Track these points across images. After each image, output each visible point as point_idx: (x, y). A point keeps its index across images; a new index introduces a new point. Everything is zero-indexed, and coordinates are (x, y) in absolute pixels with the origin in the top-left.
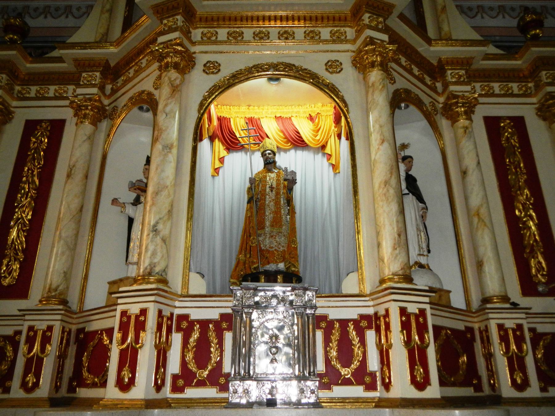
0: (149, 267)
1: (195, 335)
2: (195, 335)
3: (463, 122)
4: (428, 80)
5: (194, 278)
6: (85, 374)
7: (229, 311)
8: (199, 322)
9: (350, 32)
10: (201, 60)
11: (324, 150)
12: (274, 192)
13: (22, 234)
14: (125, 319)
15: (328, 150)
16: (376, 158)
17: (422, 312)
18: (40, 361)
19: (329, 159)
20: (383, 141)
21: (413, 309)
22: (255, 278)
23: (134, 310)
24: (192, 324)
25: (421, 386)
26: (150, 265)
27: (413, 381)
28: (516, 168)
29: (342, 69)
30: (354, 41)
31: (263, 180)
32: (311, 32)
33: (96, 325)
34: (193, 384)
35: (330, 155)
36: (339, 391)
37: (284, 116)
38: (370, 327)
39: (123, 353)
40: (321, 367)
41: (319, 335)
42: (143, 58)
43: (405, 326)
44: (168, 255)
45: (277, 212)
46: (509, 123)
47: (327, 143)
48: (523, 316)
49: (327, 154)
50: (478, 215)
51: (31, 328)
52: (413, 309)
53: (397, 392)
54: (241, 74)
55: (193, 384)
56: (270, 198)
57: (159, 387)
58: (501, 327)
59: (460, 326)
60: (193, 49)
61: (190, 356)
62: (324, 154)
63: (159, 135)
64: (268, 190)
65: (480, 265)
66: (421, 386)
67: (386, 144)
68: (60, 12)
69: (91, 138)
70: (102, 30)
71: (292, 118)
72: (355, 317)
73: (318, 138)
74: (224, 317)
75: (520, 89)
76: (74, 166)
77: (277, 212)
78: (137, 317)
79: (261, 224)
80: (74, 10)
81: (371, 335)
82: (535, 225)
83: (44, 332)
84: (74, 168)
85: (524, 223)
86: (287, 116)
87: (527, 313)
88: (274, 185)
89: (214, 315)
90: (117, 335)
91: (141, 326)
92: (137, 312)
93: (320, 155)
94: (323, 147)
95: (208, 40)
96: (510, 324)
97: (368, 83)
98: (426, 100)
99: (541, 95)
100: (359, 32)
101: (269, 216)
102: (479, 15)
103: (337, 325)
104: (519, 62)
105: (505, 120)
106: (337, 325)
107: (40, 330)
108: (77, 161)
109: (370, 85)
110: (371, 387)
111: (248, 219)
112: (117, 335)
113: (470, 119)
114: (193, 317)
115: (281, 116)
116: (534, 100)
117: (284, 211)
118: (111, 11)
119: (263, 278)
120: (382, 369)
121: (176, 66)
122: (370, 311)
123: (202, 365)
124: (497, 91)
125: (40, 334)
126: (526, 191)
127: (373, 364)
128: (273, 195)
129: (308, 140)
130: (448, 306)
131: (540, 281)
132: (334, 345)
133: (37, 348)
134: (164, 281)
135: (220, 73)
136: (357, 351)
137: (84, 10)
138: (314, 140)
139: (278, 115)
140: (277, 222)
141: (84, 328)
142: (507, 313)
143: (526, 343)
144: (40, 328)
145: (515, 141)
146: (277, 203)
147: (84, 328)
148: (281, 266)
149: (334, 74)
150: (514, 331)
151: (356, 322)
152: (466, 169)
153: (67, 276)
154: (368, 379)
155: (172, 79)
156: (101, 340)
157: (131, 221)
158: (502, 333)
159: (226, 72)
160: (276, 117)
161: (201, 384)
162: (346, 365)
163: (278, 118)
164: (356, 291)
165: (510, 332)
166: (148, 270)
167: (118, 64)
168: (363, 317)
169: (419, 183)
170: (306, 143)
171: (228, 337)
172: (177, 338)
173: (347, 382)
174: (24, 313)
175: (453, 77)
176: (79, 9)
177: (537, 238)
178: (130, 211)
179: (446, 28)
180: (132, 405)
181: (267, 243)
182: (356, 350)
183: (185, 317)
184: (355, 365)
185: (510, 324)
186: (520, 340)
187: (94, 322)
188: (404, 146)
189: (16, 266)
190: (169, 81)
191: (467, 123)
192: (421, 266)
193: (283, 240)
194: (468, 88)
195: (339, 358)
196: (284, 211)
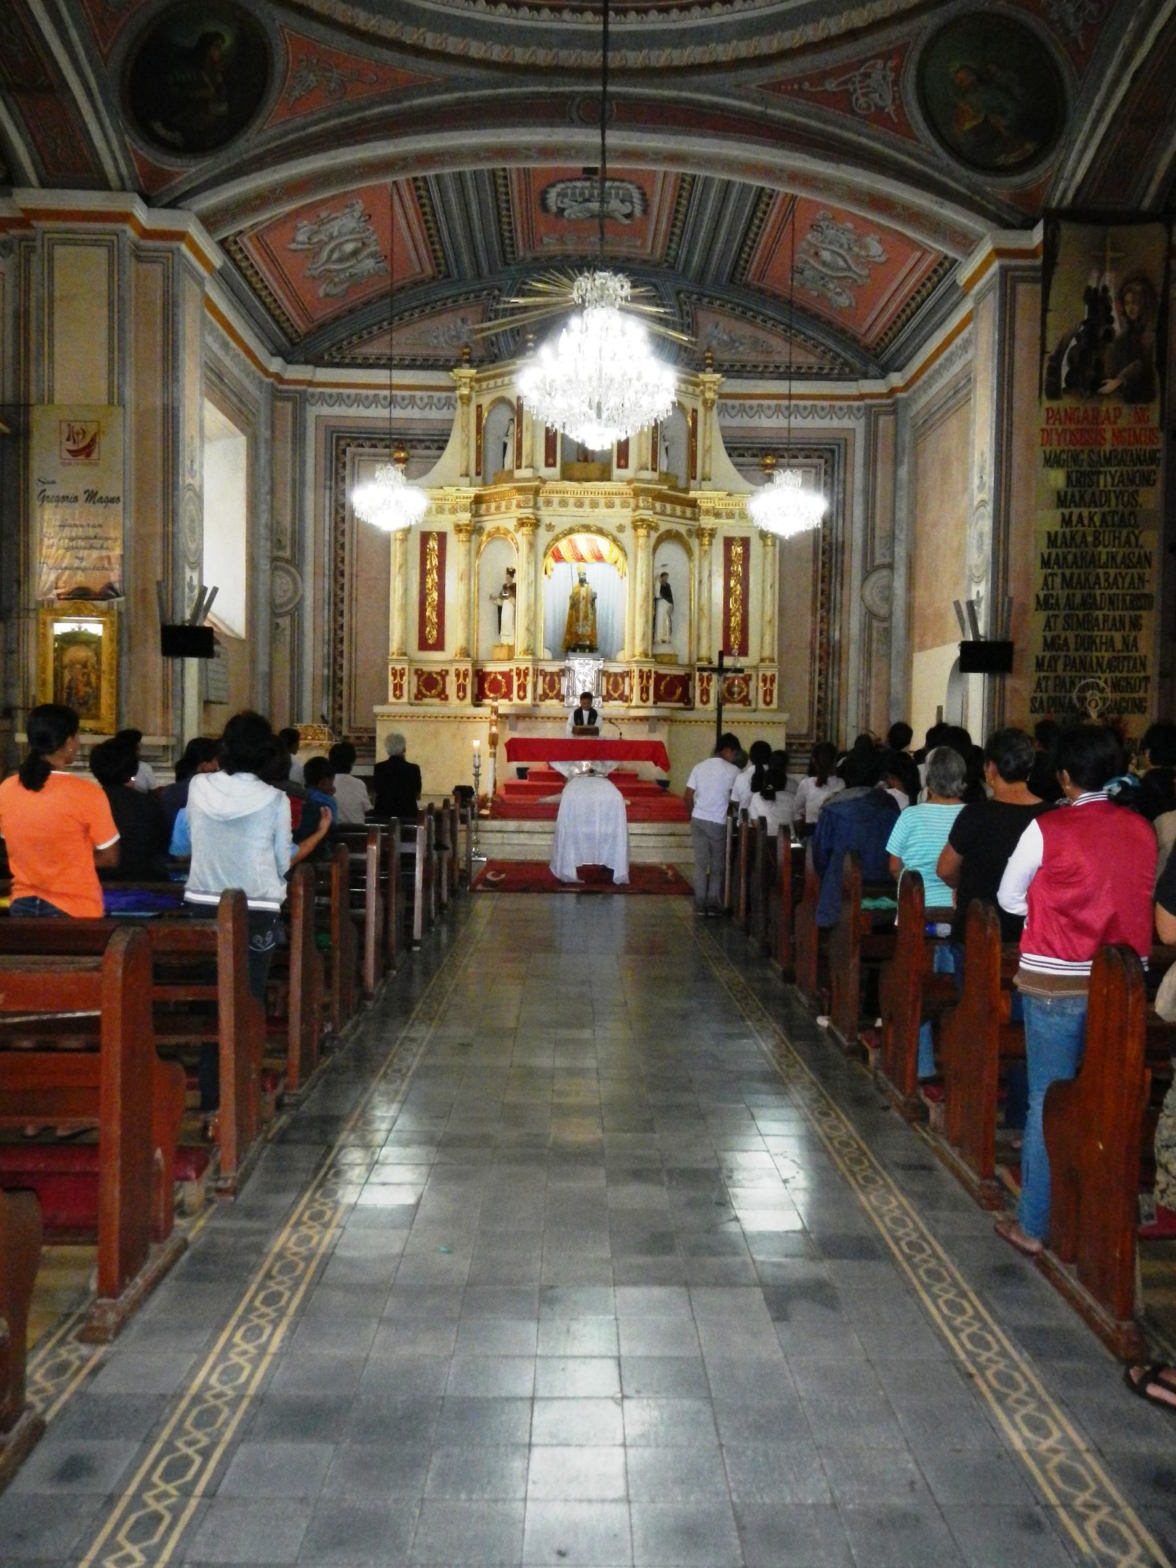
1: (548, 678)
3: (706, 548)
4: (688, 511)
5: (547, 651)
10: (546, 520)
13: (434, 614)
17: (650, 671)
21: (645, 669)
22: (574, 650)
23: (523, 667)
25: (644, 701)
27: (642, 698)
30: (634, 510)
31: (578, 593)
33: (490, 668)
36: (612, 703)
39: (519, 686)
40: (604, 693)
41: (605, 679)
43: (641, 677)
44: (535, 640)
45: (586, 612)
52: (645, 669)
53: (633, 704)
56: (582, 605)
57: (535, 699)
59: (682, 673)
60: (540, 513)
65: (699, 639)
66: (644, 701)
68: (407, 402)
69: (469, 551)
70: (464, 464)
77: (586, 612)
79: (577, 619)
80: (418, 402)
81: (627, 680)
90: (515, 678)
91: (526, 675)
95: (548, 503)
98: (683, 530)
100: (637, 507)
101: (582, 614)
102: (757, 417)
110: (626, 701)
111: (570, 616)
112: (515, 678)
113: (710, 544)
117: (590, 611)
118: (468, 445)
123: (552, 691)
127: (627, 692)
130: (676, 664)
134: (533, 654)
136: (621, 687)
137: (426, 400)
140: (586, 617)
146: (586, 606)
148: (588, 643)
153: (468, 640)
156: (495, 678)
157: (500, 609)
159: (557, 531)
162: (615, 691)
169: (673, 589)
172: (541, 679)
173: (615, 699)
174: (451, 662)
176: (421, 399)
178: (499, 602)
179: (707, 469)
180: (528, 708)
181: (580, 631)
183: (542, 670)
188: (664, 566)
189: (435, 632)
191: (706, 548)
192: (664, 642)
193: (589, 629)
196: (590, 611)
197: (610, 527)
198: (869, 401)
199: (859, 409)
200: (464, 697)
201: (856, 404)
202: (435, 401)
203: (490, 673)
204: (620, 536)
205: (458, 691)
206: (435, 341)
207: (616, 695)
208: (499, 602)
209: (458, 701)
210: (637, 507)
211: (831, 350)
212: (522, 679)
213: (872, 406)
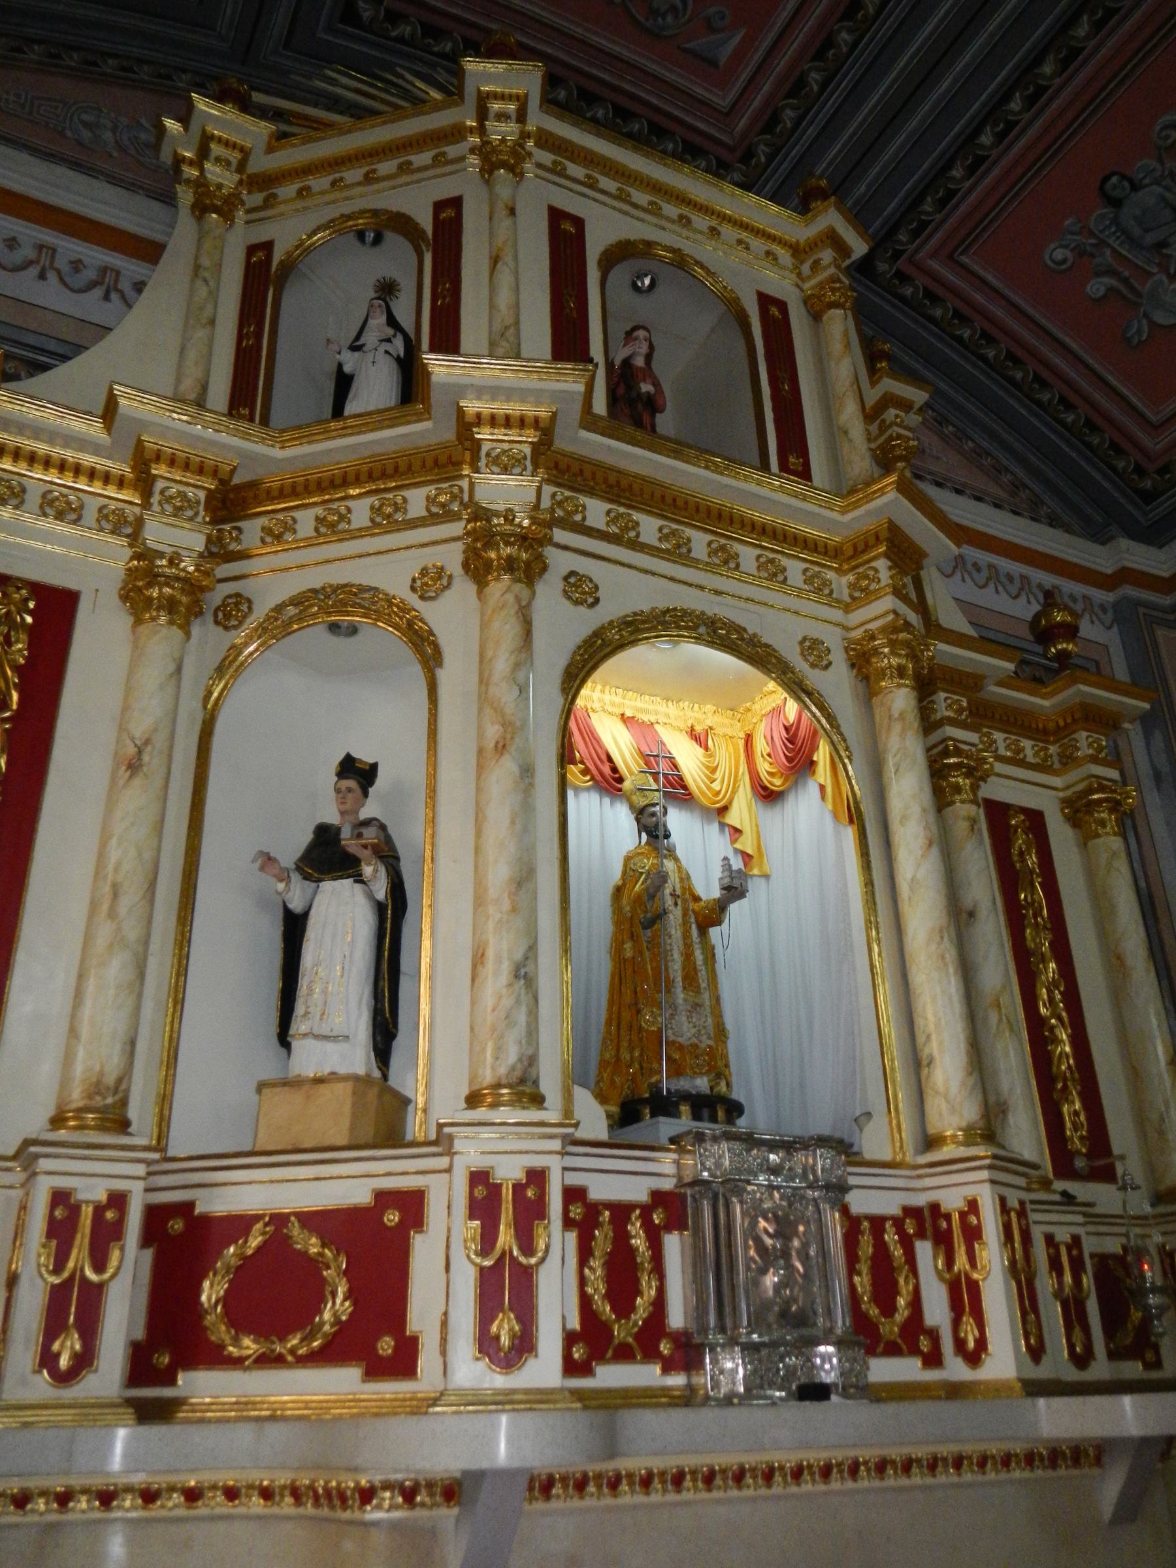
0: (519, 1066)
2: (602, 1238)
6: (220, 1332)
7: (667, 1185)
8: (610, 1206)
9: (841, 583)
11: (724, 817)
12: (679, 907)
14: (480, 1192)
15: (733, 818)
16: (919, 876)
18: (93, 1296)
19: (733, 841)
20: (930, 845)
24: (593, 1210)
26: (520, 1060)
28: (1035, 917)
29: (830, 663)
32: (772, 561)
34: (610, 1353)
35: (737, 831)
37: (645, 718)
38: (921, 1234)
42: (360, 496)
45: (688, 956)
46: (1023, 821)
47: (731, 802)
48: (1080, 1219)
49: (729, 826)
50: (999, 1006)
51: (60, 1197)
54: (644, 622)
55: (610, 1353)
58: (1050, 1239)
61: (597, 1287)
62: (722, 825)
63: (508, 736)
64: (669, 901)
67: (935, 851)
71: (656, 726)
72: (894, 1210)
73: (716, 786)
74: (659, 1198)
75: (1036, 754)
76: (147, 742)
77: (688, 956)
78: (518, 1188)
82: (1068, 1036)
83: (99, 1210)
84: (149, 748)
85: (1052, 1028)
86: (646, 720)
87: (1085, 1215)
88: (678, 892)
89: (635, 1191)
92: (519, 1175)
93: (715, 826)
94: (724, 810)
96: (1063, 1235)
97: (890, 710)
99: (1074, 775)
103: (866, 1224)
104: (1046, 703)
105: (1017, 812)
106: (866, 1224)
107: (87, 1202)
108: (156, 730)
109: (896, 715)
114: (595, 1195)
115: (633, 718)
116: (1057, 781)
119: (685, 1109)
120: (956, 1323)
121: (510, 565)
122: (920, 1200)
124: (1030, 759)
125: (87, 1212)
126: (1052, 965)
128: (678, 912)
129: (698, 787)
131: (1078, 1152)
132: (864, 1267)
133: (79, 1256)
135: (598, 608)
138: (709, 788)
139: (628, 714)
141: (190, 1205)
142: (1058, 1212)
143: (1085, 1272)
144: (81, 1196)
145: (1032, 860)
147: (190, 1205)
149: (817, 671)
150: (1069, 1248)
151: (898, 1223)
152: (975, 906)
154: (924, 1344)
155: (524, 603)
158: (1051, 1251)
159: (610, 609)
160: (623, 715)
161: (624, 1354)
163: (625, 720)
164: (887, 1156)
165: (1063, 1251)
166: (518, 1073)
167: (253, 485)
168: (911, 1211)
170: (690, 794)
171: (673, 1243)
175: (949, 707)
177: (1071, 1061)
182: (901, 1281)
184: (902, 1314)
185: (1063, 1235)
186: (1077, 1266)
187: (215, 1190)
190: (516, 607)
194: (973, 737)
195: (876, 1298)
197: (785, 642)
198: (1130, 591)
199: (1103, 608)
200: (84, 1361)
201: (1099, 596)
202: (61, 263)
203: (240, 1224)
204: (814, 678)
205: (53, 1327)
206: (86, 134)
207: (890, 1329)
208: (297, 895)
209: (42, 1386)
210: (862, 595)
211: (1025, 486)
212: (505, 1237)
213: (1139, 603)
